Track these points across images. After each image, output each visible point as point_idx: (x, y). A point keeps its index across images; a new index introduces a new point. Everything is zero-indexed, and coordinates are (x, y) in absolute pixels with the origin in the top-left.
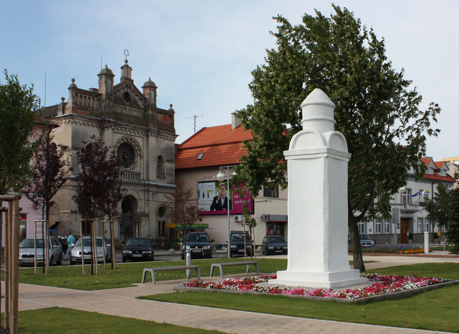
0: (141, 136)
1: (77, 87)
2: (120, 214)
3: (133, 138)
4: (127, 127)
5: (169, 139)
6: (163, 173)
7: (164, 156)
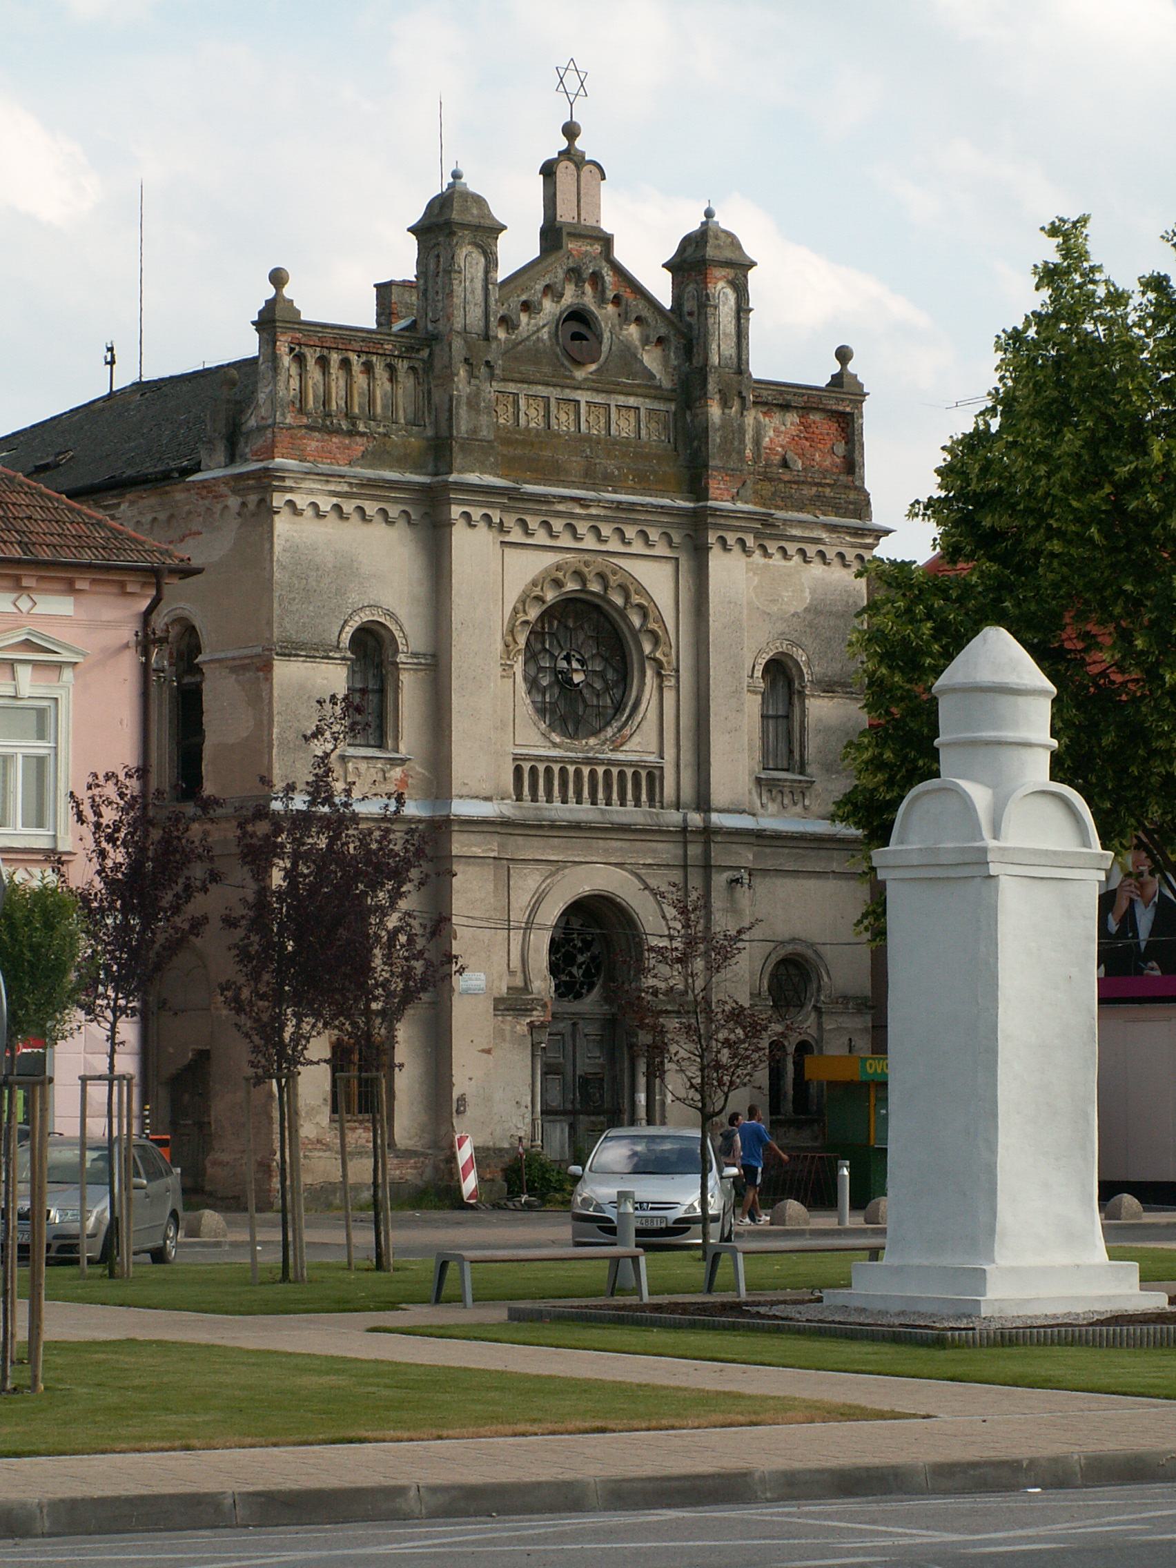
0: (661, 550)
1: (298, 312)
2: (544, 1006)
3: (618, 570)
4: (578, 510)
5: (831, 553)
6: (797, 757)
7: (801, 657)
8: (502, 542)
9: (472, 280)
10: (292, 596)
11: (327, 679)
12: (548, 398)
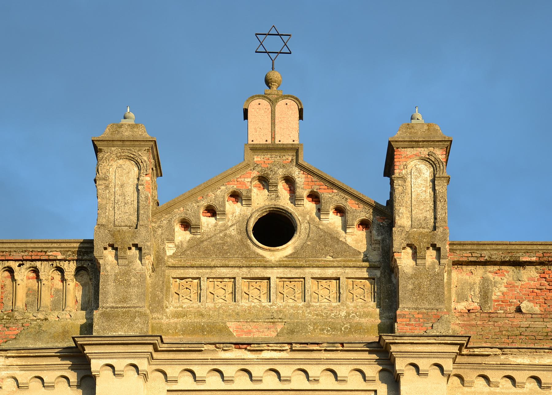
8: (168, 391)
9: (122, 186)
12: (234, 278)
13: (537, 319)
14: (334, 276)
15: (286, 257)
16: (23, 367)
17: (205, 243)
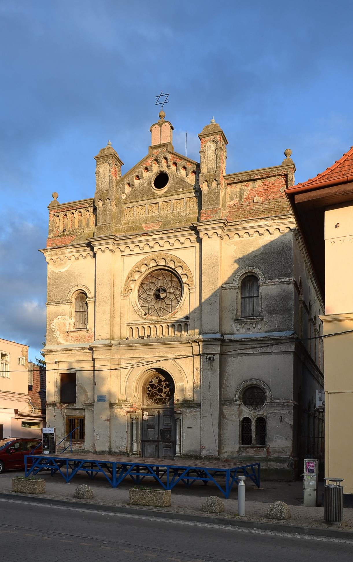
0: (188, 243)
4: (148, 238)
5: (271, 229)
8: (122, 256)
10: (52, 287)
11: (63, 310)
13: (260, 205)
14: (182, 198)
15: (165, 192)
16: (76, 252)
17: (136, 191)
